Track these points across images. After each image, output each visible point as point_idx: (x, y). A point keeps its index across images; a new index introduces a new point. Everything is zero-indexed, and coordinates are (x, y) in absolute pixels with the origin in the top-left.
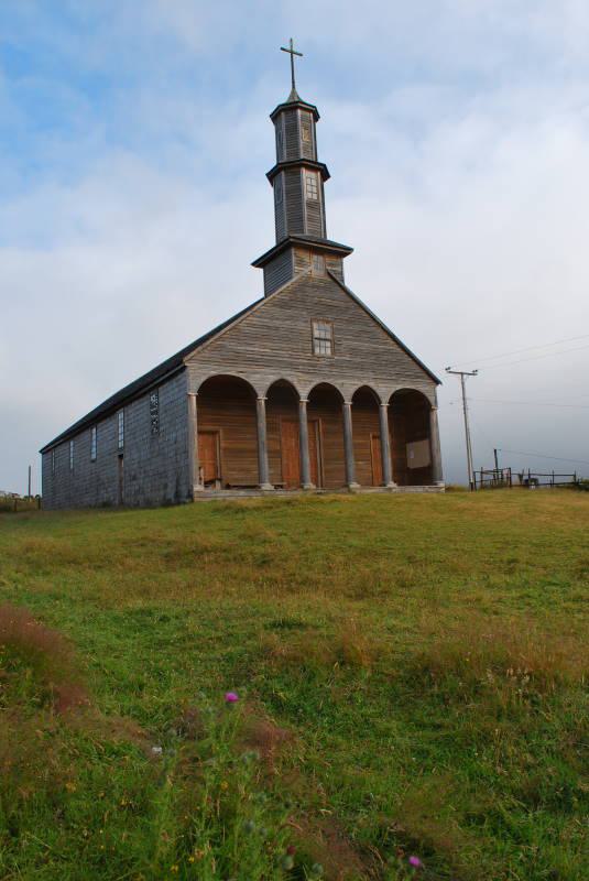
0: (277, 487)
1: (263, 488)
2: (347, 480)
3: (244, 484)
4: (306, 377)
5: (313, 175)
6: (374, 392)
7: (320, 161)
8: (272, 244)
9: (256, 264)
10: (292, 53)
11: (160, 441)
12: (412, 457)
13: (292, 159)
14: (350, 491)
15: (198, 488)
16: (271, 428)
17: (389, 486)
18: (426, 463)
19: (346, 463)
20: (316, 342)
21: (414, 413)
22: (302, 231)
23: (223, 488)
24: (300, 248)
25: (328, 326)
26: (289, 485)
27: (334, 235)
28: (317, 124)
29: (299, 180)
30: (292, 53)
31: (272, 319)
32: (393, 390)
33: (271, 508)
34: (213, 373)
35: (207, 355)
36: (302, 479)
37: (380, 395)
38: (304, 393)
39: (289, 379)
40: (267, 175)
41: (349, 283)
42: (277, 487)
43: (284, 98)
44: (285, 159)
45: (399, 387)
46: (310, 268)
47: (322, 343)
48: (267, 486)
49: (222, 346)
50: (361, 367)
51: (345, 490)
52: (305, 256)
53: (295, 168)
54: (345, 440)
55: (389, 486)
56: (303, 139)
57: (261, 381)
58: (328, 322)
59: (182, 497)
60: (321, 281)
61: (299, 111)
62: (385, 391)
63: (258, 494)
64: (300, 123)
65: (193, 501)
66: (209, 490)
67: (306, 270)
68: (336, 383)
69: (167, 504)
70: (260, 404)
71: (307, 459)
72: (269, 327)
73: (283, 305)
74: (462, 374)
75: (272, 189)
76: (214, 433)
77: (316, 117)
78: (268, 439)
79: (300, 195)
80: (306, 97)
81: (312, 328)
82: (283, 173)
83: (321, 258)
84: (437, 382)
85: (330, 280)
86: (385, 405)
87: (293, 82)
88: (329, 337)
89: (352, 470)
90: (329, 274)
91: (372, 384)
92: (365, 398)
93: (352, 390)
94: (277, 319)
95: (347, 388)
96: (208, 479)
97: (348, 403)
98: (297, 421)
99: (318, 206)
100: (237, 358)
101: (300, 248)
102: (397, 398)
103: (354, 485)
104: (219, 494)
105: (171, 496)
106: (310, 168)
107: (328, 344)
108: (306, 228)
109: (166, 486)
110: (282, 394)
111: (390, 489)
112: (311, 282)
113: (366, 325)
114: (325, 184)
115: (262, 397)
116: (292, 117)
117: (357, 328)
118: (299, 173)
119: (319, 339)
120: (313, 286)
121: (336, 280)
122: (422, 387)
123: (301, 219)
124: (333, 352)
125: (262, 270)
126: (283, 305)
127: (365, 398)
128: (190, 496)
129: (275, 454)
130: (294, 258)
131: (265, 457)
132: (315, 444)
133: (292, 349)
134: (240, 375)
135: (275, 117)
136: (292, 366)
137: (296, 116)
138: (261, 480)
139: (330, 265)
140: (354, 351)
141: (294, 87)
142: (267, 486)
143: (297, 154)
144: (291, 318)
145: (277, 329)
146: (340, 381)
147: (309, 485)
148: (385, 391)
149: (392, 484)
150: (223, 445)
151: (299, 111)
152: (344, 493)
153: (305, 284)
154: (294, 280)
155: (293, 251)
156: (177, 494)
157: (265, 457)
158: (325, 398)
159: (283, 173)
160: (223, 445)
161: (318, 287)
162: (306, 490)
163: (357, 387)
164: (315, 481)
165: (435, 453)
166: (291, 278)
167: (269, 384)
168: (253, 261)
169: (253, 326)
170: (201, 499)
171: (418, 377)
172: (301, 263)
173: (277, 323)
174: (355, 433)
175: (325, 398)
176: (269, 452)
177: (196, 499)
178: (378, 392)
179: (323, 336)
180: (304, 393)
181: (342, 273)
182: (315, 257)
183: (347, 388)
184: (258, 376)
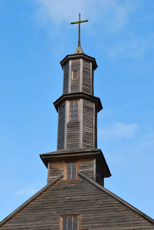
31: (26, 221)
85: (81, 180)
87: (79, 42)
94: (30, 222)
101: (79, 160)
112: (63, 186)
113: (116, 210)
120: (65, 188)
139: (85, 167)
141: (79, 42)
144: (43, 218)
151: (70, 62)
161: (68, 188)
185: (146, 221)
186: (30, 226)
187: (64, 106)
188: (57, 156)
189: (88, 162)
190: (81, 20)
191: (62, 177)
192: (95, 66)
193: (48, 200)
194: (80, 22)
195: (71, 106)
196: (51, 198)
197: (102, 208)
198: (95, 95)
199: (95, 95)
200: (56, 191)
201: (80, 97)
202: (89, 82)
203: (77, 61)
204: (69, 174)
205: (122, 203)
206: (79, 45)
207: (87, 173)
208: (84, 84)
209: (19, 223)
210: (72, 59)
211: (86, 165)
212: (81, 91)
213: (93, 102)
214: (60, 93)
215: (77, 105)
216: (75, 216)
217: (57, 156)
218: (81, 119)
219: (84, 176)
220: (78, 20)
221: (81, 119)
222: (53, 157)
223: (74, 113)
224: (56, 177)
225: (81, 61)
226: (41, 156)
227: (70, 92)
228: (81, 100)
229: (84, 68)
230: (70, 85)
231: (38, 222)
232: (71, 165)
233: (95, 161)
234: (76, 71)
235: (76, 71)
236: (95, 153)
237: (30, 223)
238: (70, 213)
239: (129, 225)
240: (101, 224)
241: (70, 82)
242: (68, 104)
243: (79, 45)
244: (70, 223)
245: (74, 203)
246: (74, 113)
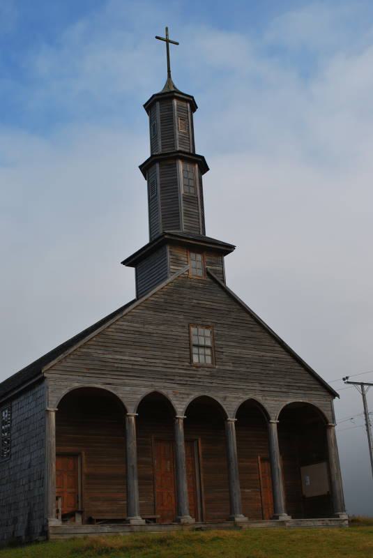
0: (148, 521)
1: (133, 522)
2: (232, 511)
3: (110, 518)
4: (183, 390)
5: (188, 166)
6: (262, 407)
7: (197, 153)
8: (145, 240)
9: (127, 262)
10: (168, 41)
11: (11, 465)
12: (308, 483)
13: (167, 150)
14: (237, 526)
15: (54, 522)
16: (141, 450)
17: (281, 518)
18: (325, 490)
19: (230, 492)
20: (195, 350)
21: (308, 429)
22: (178, 227)
23: (84, 522)
25: (208, 333)
26: (163, 519)
27: (213, 231)
28: (194, 114)
29: (175, 173)
30: (168, 41)
32: (284, 404)
33: (140, 548)
34: (76, 385)
35: (69, 364)
36: (179, 512)
37: (269, 410)
38: (180, 408)
39: (164, 392)
40: (140, 167)
41: (231, 283)
42: (148, 521)
43: (159, 88)
44: (160, 151)
45: (290, 401)
46: (188, 267)
47: (201, 350)
48: (137, 520)
49: (87, 354)
51: (229, 524)
52: (182, 255)
53: (173, 165)
54: (229, 465)
55: (281, 518)
56: (179, 130)
57: (131, 394)
58: (207, 327)
59: (36, 534)
60: (199, 281)
61: (175, 102)
62: (274, 406)
63: (127, 529)
64: (176, 113)
65: (47, 539)
66: (68, 526)
67: (182, 270)
68: (218, 396)
69: (15, 543)
70: (130, 421)
71: (184, 487)
72: (141, 333)
73: (156, 307)
74: (362, 384)
75: (146, 182)
76: (75, 456)
77: (194, 107)
78: (139, 462)
79: (176, 190)
80: (182, 87)
81: (189, 333)
82: (157, 165)
83: (199, 257)
84: (333, 394)
85: (209, 280)
86: (274, 422)
87: (169, 71)
88: (209, 343)
89: (237, 499)
90: (208, 274)
91: (259, 398)
92: (252, 413)
94: (150, 324)
95: (231, 404)
96: (68, 510)
97: (232, 419)
98: (172, 440)
99: (196, 200)
102: (288, 413)
103: (240, 518)
104: (80, 530)
105: (21, 533)
106: (184, 159)
107: (208, 352)
108: (183, 224)
109: (15, 520)
111: (283, 523)
114: (203, 176)
115: (132, 413)
118: (175, 166)
119: (198, 346)
120: (191, 287)
121: (216, 280)
122: (316, 400)
123: (177, 215)
124: (214, 360)
125: (132, 270)
126: (156, 307)
127: (252, 413)
128: (45, 533)
129: (145, 480)
130: (169, 256)
131: (134, 484)
132: (194, 467)
133: (167, 358)
134: (108, 388)
135: (149, 107)
137: (172, 106)
138: (129, 512)
139: (211, 264)
140: (237, 360)
141: (169, 71)
142: (137, 520)
143: (173, 145)
145: (150, 334)
146: (221, 394)
147: (188, 519)
148: (274, 406)
149: (285, 517)
150: (85, 470)
151: (175, 102)
152: (230, 528)
153: (183, 283)
154: (168, 281)
155: (168, 249)
156: (29, 531)
157: (134, 484)
159: (157, 165)
160: (85, 470)
162: (183, 524)
163: (241, 401)
164: (194, 514)
165: (334, 478)
166: (167, 278)
167: (140, 397)
168: (123, 260)
169: (123, 331)
170: (57, 537)
171: (312, 389)
172: (177, 261)
173: (150, 328)
174: (240, 455)
175: (205, 413)
176: (140, 478)
177: (52, 537)
178: (265, 406)
179: (202, 343)
180: (180, 408)
181: (223, 273)
182: (193, 255)
183: (231, 404)
185: (282, 349)
186: (152, 331)
188: (184, 240)
193: (172, 298)
197: (235, 324)
200: (181, 289)
203: (184, 104)
209: (137, 323)
210: (178, 98)
211: (213, 261)
217: (184, 240)
219: (213, 275)
222: (179, 239)
231: (162, 327)
236: (173, 238)
237: (151, 327)
238: (201, 323)
239: (265, 351)
245: (204, 310)
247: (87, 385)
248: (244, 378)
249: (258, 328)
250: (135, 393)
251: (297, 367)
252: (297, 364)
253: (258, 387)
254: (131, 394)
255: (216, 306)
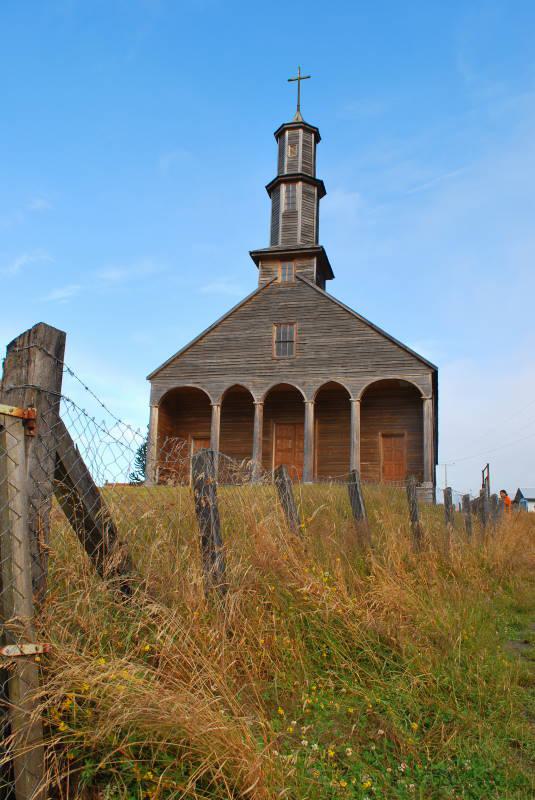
4: (258, 380)
21: (403, 402)
24: (297, 258)
32: (370, 383)
38: (258, 397)
39: (245, 384)
50: (329, 363)
57: (214, 391)
60: (288, 284)
62: (355, 386)
87: (298, 106)
93: (316, 387)
100: (195, 371)
101: (297, 258)
110: (237, 401)
112: (277, 289)
116: (300, 134)
117: (324, 324)
120: (280, 292)
133: (250, 356)
136: (247, 371)
141: (298, 106)
144: (252, 326)
145: (236, 339)
146: (300, 381)
148: (355, 386)
151: (287, 133)
158: (284, 402)
163: (320, 384)
167: (223, 390)
169: (213, 340)
171: (403, 365)
175: (284, 402)
180: (258, 397)
184: (213, 384)
185: (372, 332)
187: (279, 191)
189: (308, 261)
190: (302, 76)
191: (276, 279)
192: (318, 139)
194: (300, 79)
195: (288, 191)
196: (263, 304)
198: (317, 177)
199: (318, 177)
201: (299, 180)
202: (310, 159)
203: (295, 132)
204: (284, 275)
205: (346, 311)
206: (298, 110)
207: (305, 275)
208: (303, 162)
212: (299, 171)
213: (315, 185)
214: (273, 175)
215: (294, 190)
216: (292, 324)
218: (299, 207)
219: (301, 277)
220: (297, 76)
221: (299, 207)
223: (291, 201)
224: (269, 279)
225: (301, 131)
226: (251, 253)
227: (286, 173)
228: (300, 183)
229: (304, 141)
230: (286, 163)
232: (287, 264)
233: (315, 260)
234: (293, 145)
235: (293, 145)
239: (353, 336)
240: (321, 334)
241: (286, 160)
242: (283, 188)
243: (298, 110)
244: (285, 334)
246: (291, 201)
247: (182, 385)
248: (319, 363)
249: (347, 316)
250: (220, 387)
251: (390, 346)
252: (389, 343)
253: (341, 370)
254: (214, 391)
255: (303, 304)
